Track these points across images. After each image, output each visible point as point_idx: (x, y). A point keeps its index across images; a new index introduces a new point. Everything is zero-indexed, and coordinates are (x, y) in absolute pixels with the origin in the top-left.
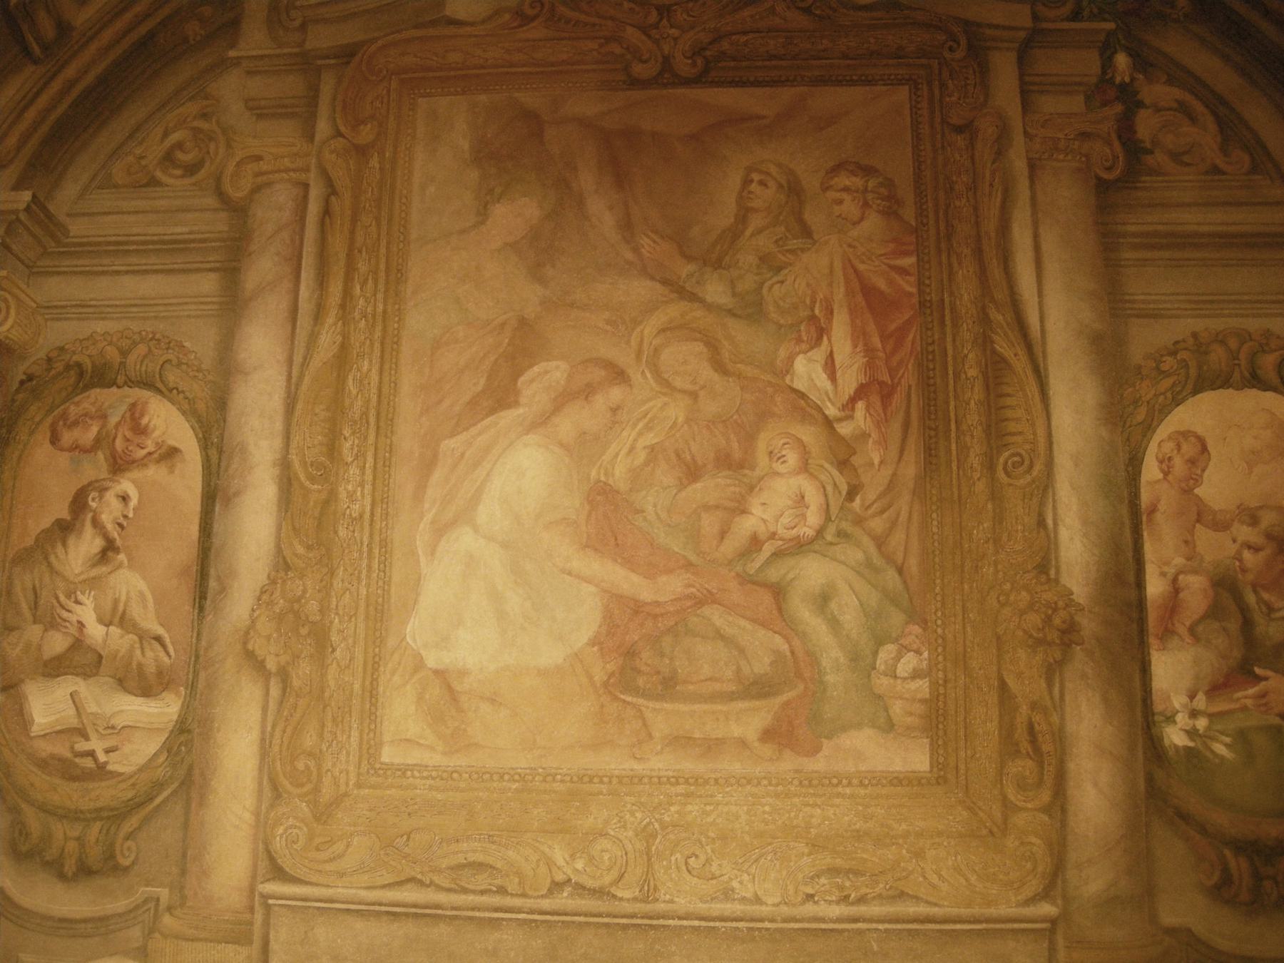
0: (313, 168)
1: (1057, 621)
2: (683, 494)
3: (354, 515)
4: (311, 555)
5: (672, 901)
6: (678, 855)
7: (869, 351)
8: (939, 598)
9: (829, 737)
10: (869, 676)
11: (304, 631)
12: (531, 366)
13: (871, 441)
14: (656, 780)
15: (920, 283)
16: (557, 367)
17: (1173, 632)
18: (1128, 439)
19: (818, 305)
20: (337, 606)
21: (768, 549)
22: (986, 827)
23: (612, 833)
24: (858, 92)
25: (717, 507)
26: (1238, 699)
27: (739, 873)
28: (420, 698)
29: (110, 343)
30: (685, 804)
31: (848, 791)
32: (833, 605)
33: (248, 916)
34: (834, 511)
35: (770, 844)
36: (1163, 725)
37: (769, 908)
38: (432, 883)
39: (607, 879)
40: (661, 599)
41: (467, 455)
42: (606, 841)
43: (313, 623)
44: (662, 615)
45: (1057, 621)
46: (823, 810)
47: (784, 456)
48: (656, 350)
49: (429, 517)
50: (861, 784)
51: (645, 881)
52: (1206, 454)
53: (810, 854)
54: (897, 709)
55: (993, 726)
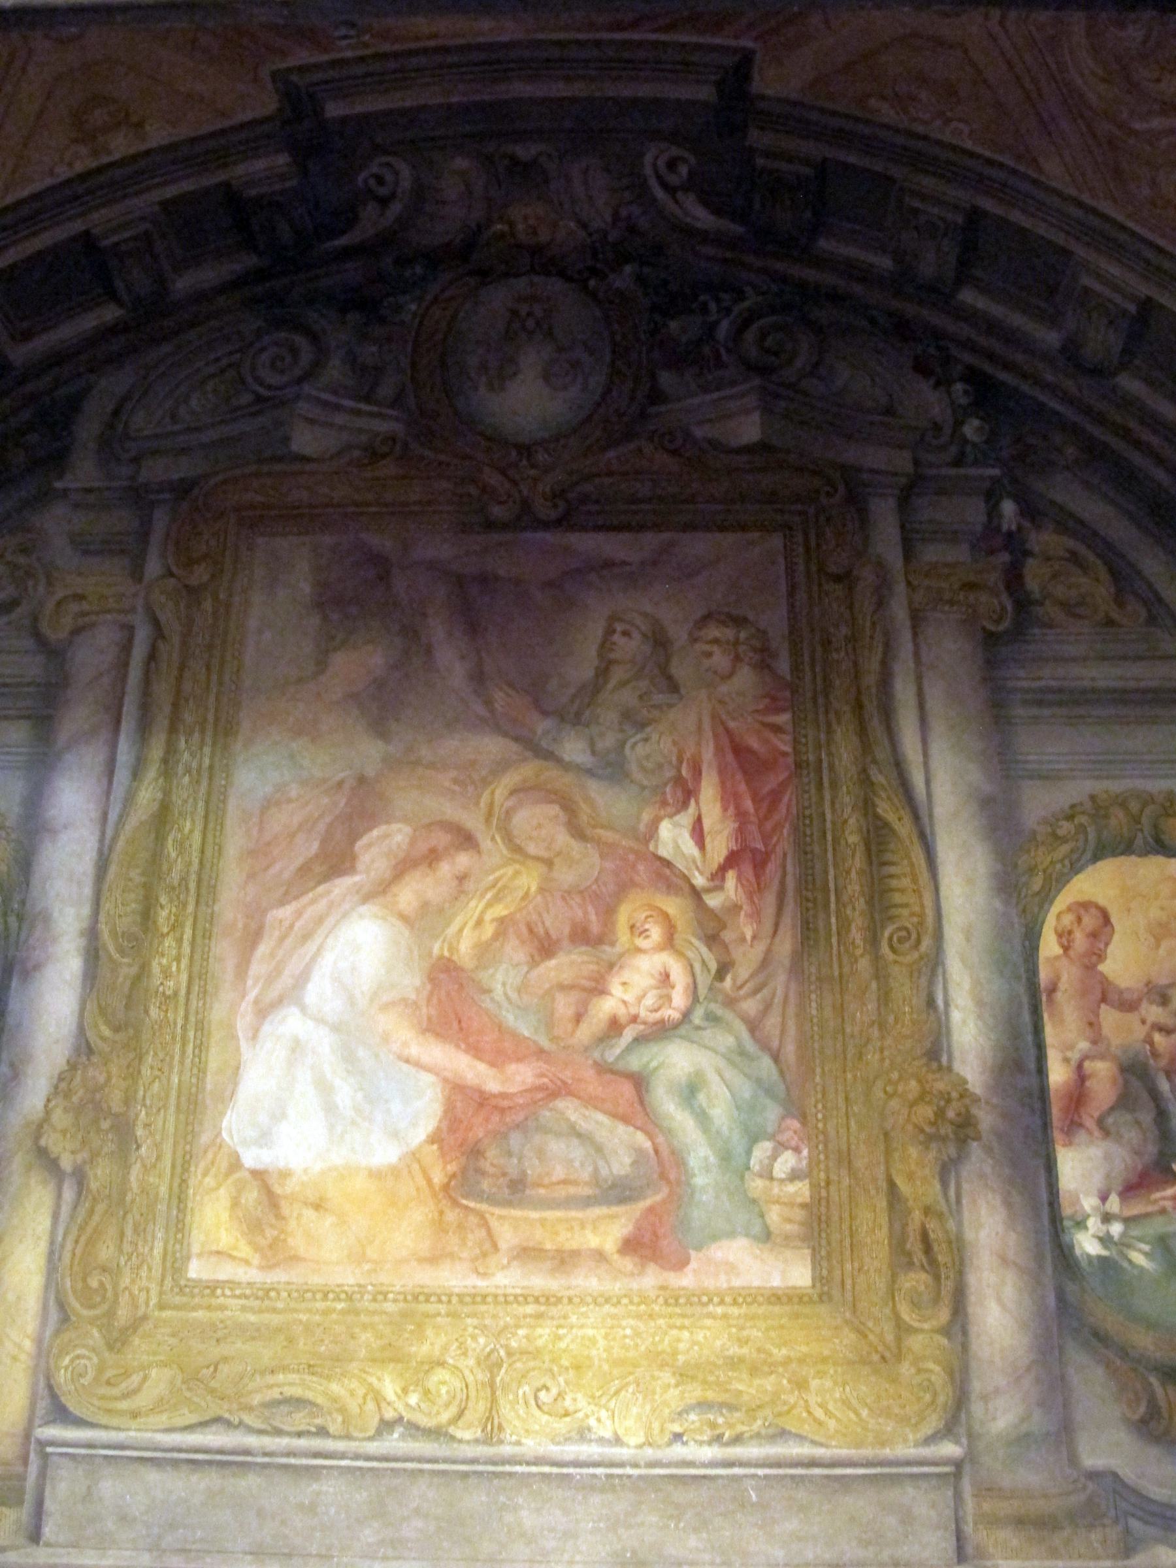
0: (140, 610)
1: (951, 1114)
2: (535, 973)
3: (168, 993)
4: (118, 1037)
5: (518, 1443)
6: (526, 1388)
7: (741, 815)
8: (819, 1088)
9: (699, 1248)
10: (742, 1178)
11: (105, 1125)
12: (370, 829)
13: (743, 913)
14: (502, 1299)
15: (796, 741)
16: (400, 830)
17: (1081, 1125)
18: (1024, 911)
19: (684, 765)
20: (144, 1096)
21: (629, 1034)
22: (877, 1351)
23: (451, 1361)
24: (729, 539)
25: (572, 987)
26: (1156, 1201)
27: (595, 1409)
28: (235, 1203)
30: (533, 1327)
31: (720, 1310)
32: (701, 1097)
33: (19, 1469)
34: (702, 991)
35: (631, 1373)
36: (1073, 1231)
37: (632, 1451)
38: (241, 1423)
39: (445, 1417)
40: (512, 1090)
41: (296, 928)
42: (444, 1372)
43: (117, 1115)
44: (510, 1108)
45: (951, 1114)
46: (692, 1333)
47: (646, 930)
48: (507, 812)
49: (252, 995)
50: (735, 1302)
51: (488, 1419)
52: (1108, 928)
53: (677, 1386)
54: (774, 1216)
55: (883, 1234)
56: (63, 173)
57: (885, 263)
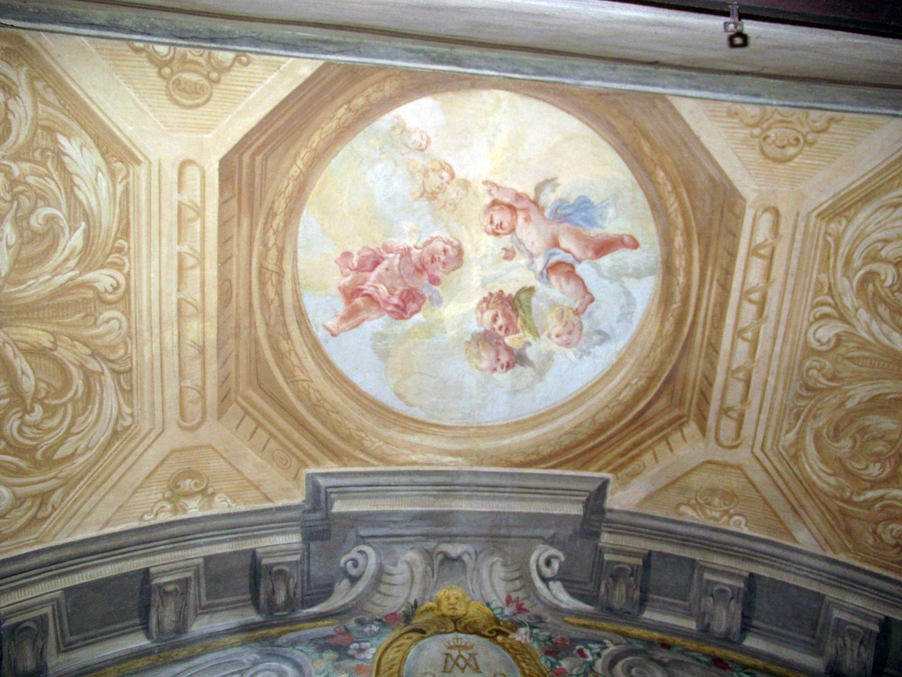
56: (150, 520)
57: (691, 625)
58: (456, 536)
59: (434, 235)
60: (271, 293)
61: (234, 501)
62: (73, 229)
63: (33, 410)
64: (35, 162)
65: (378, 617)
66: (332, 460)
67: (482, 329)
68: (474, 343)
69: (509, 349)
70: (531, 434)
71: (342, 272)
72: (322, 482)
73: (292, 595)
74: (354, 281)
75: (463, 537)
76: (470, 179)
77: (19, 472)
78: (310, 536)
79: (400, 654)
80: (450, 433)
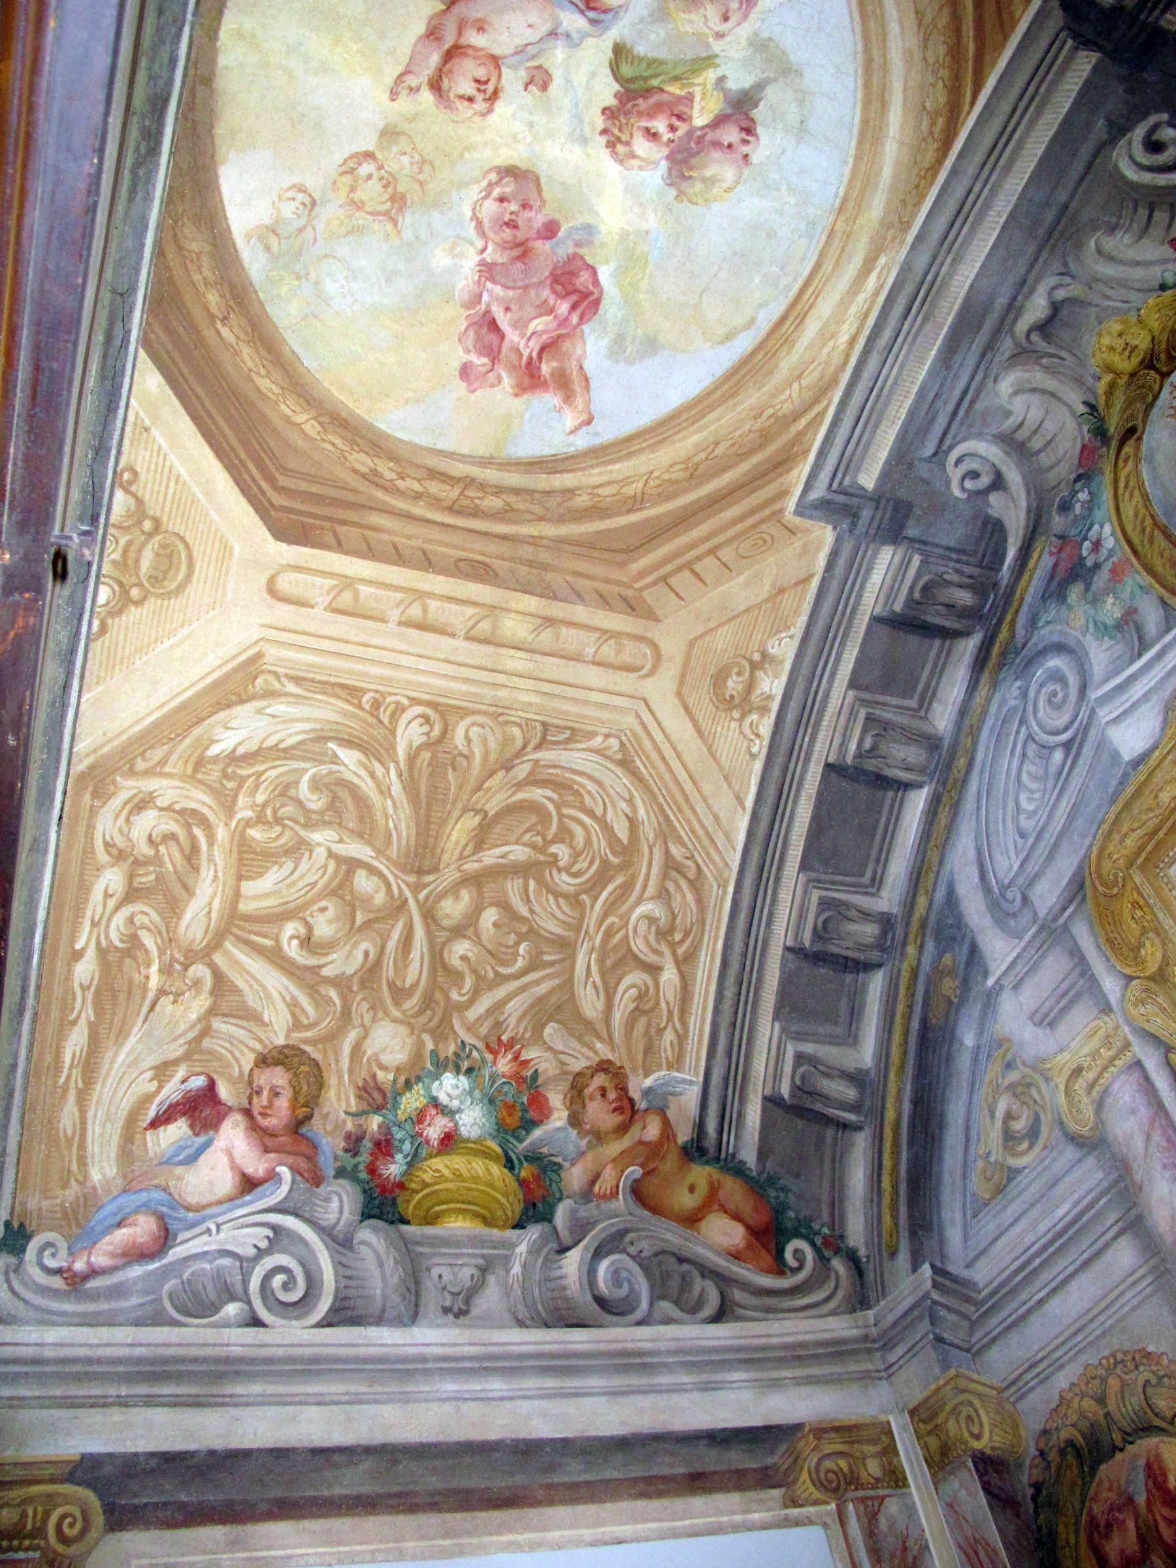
29: (1083, 1395)
56: (760, 747)
58: (1014, 299)
59: (469, 214)
60: (492, 503)
61: (787, 628)
62: (335, 759)
63: (555, 856)
64: (240, 787)
65: (1073, 476)
66: (791, 469)
67: (664, 164)
68: (684, 185)
69: (719, 122)
70: (895, 117)
71: (492, 386)
72: (816, 494)
73: (970, 581)
74: (512, 368)
75: (1023, 288)
76: (381, 124)
77: (627, 887)
78: (893, 533)
79: (1136, 493)
80: (828, 266)
